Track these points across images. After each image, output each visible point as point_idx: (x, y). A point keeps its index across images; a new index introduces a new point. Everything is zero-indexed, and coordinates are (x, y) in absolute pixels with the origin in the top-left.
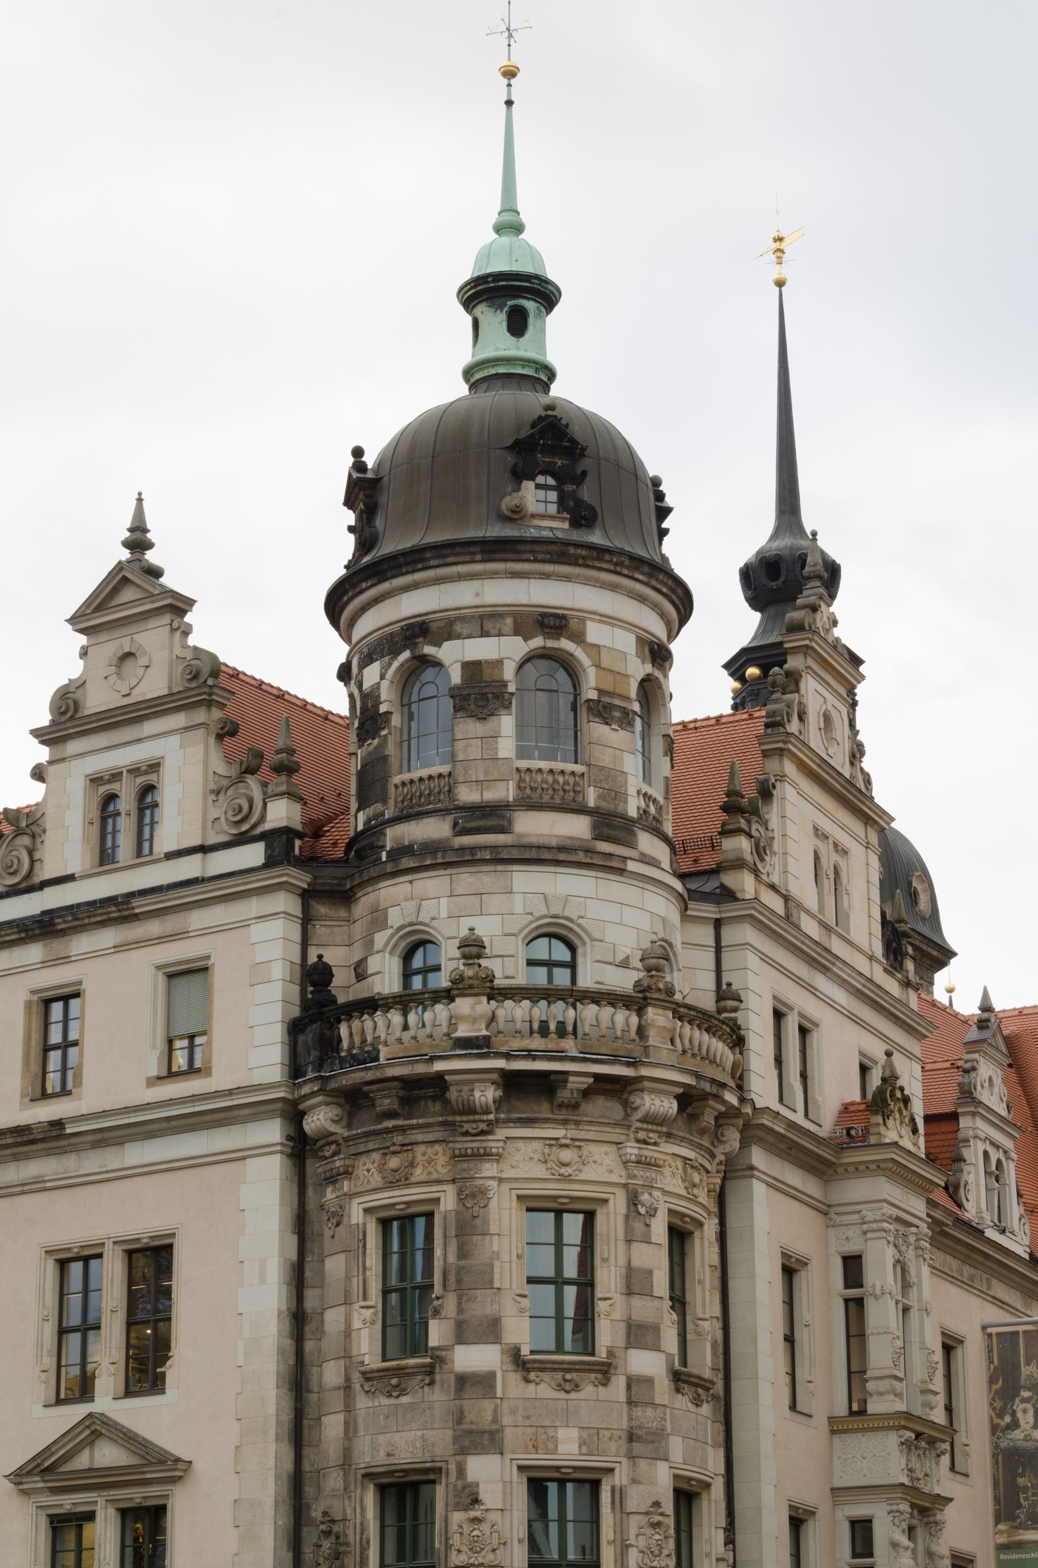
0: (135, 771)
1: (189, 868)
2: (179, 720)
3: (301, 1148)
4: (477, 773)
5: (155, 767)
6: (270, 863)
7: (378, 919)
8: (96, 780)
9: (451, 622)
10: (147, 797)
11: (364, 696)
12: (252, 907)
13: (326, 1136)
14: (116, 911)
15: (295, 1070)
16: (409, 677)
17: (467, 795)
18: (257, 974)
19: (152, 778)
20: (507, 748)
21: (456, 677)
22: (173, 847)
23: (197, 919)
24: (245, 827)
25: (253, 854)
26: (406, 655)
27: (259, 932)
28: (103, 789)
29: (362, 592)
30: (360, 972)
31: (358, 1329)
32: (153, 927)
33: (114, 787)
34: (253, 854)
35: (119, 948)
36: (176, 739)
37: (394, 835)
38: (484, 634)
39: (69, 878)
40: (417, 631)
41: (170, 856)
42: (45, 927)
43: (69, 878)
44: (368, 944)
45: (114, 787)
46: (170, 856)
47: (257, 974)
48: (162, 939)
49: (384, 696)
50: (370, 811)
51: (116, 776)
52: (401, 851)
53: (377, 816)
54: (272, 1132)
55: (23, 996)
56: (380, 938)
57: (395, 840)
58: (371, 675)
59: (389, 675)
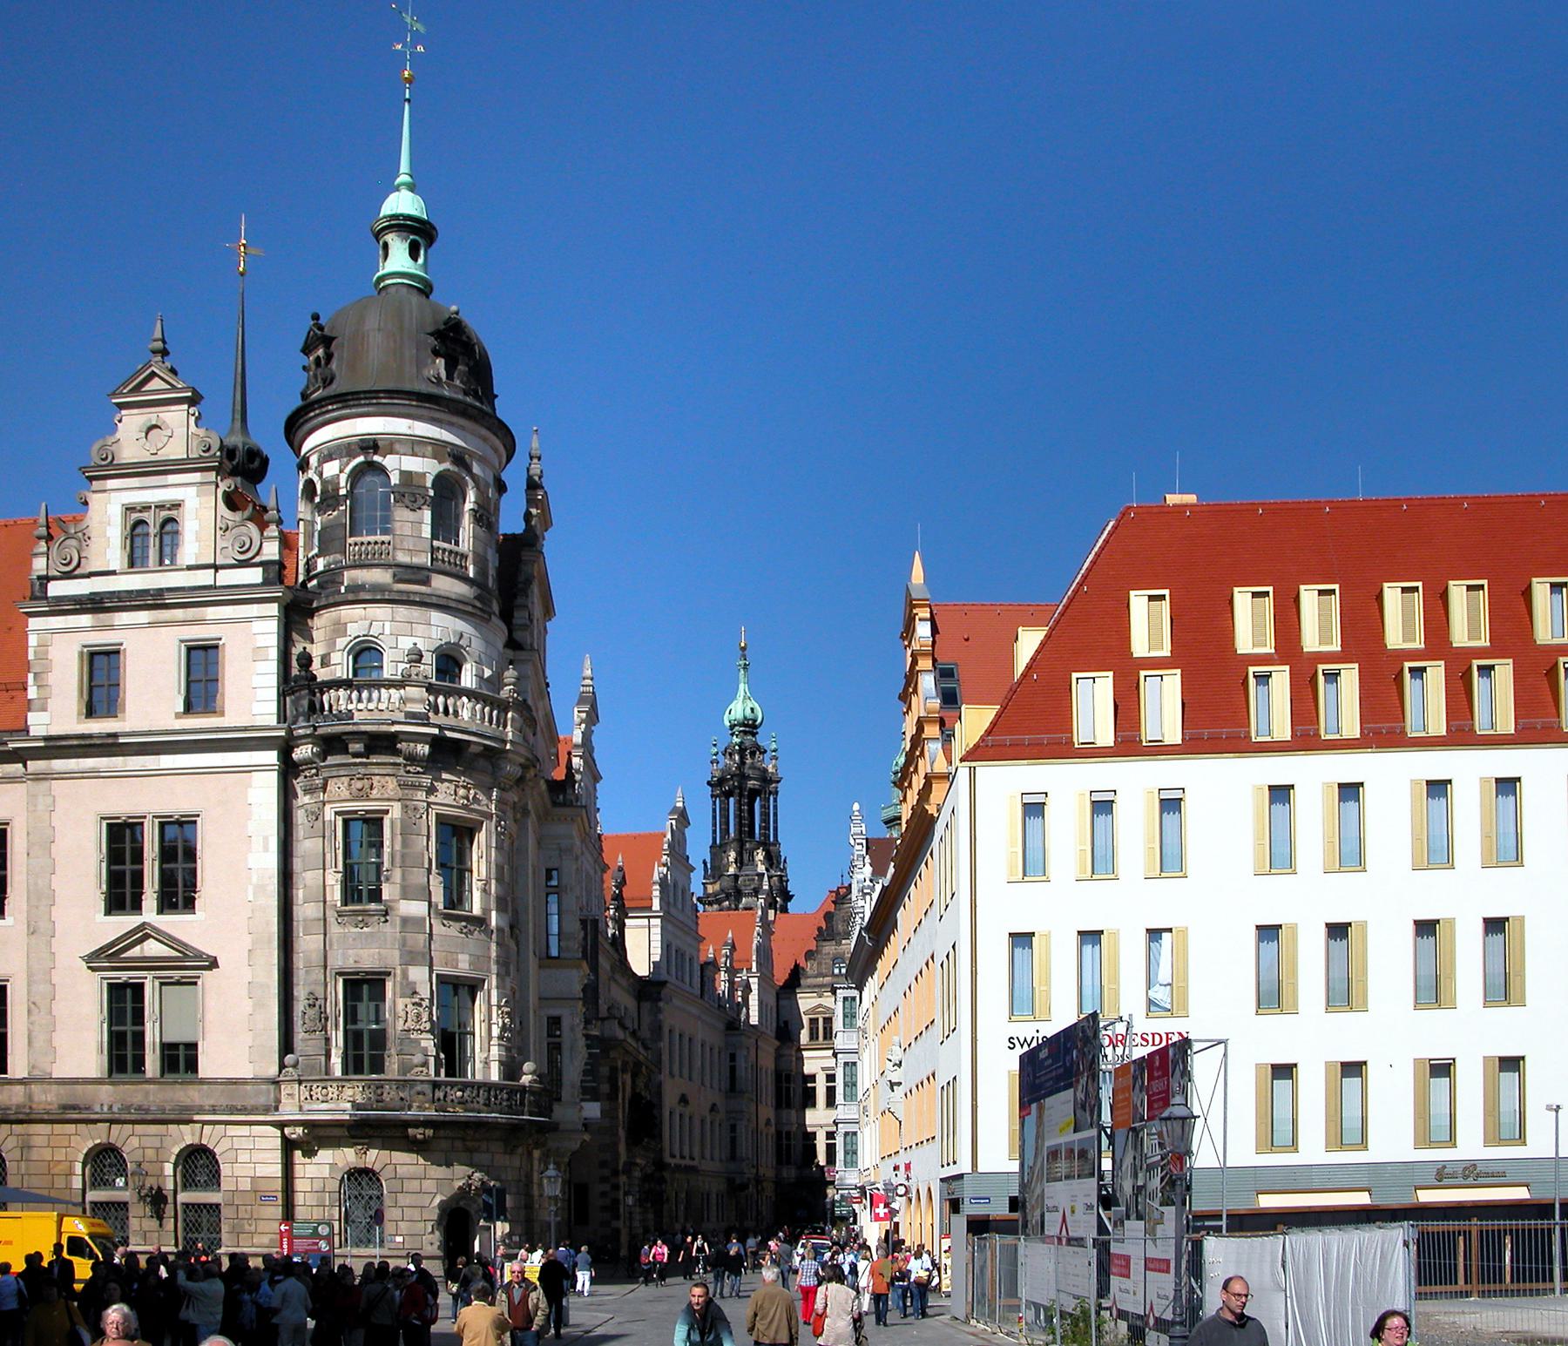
0: (160, 507)
1: (205, 578)
2: (197, 477)
3: (289, 770)
4: (408, 544)
5: (177, 506)
6: (266, 582)
7: (340, 628)
8: (129, 509)
9: (392, 443)
10: (170, 526)
11: (324, 482)
12: (254, 610)
13: (307, 762)
14: (153, 600)
15: (282, 716)
16: (356, 476)
17: (402, 558)
18: (258, 654)
19: (173, 513)
20: (427, 531)
21: (395, 479)
22: (193, 562)
23: (211, 612)
24: (250, 555)
25: (254, 575)
26: (361, 459)
27: (258, 626)
28: (135, 516)
29: (328, 412)
30: (325, 662)
31: (321, 880)
32: (179, 614)
33: (144, 516)
34: (254, 575)
35: (152, 625)
36: (193, 490)
37: (348, 576)
38: (414, 454)
39: (113, 573)
40: (371, 445)
41: (190, 568)
42: (95, 604)
43: (113, 573)
44: (331, 644)
45: (144, 516)
46: (190, 568)
47: (258, 654)
48: (184, 623)
49: (342, 484)
50: (331, 558)
51: (146, 508)
52: (355, 588)
53: (335, 563)
54: (271, 757)
55: (77, 648)
56: (341, 642)
57: (351, 579)
58: (331, 469)
59: (348, 470)
